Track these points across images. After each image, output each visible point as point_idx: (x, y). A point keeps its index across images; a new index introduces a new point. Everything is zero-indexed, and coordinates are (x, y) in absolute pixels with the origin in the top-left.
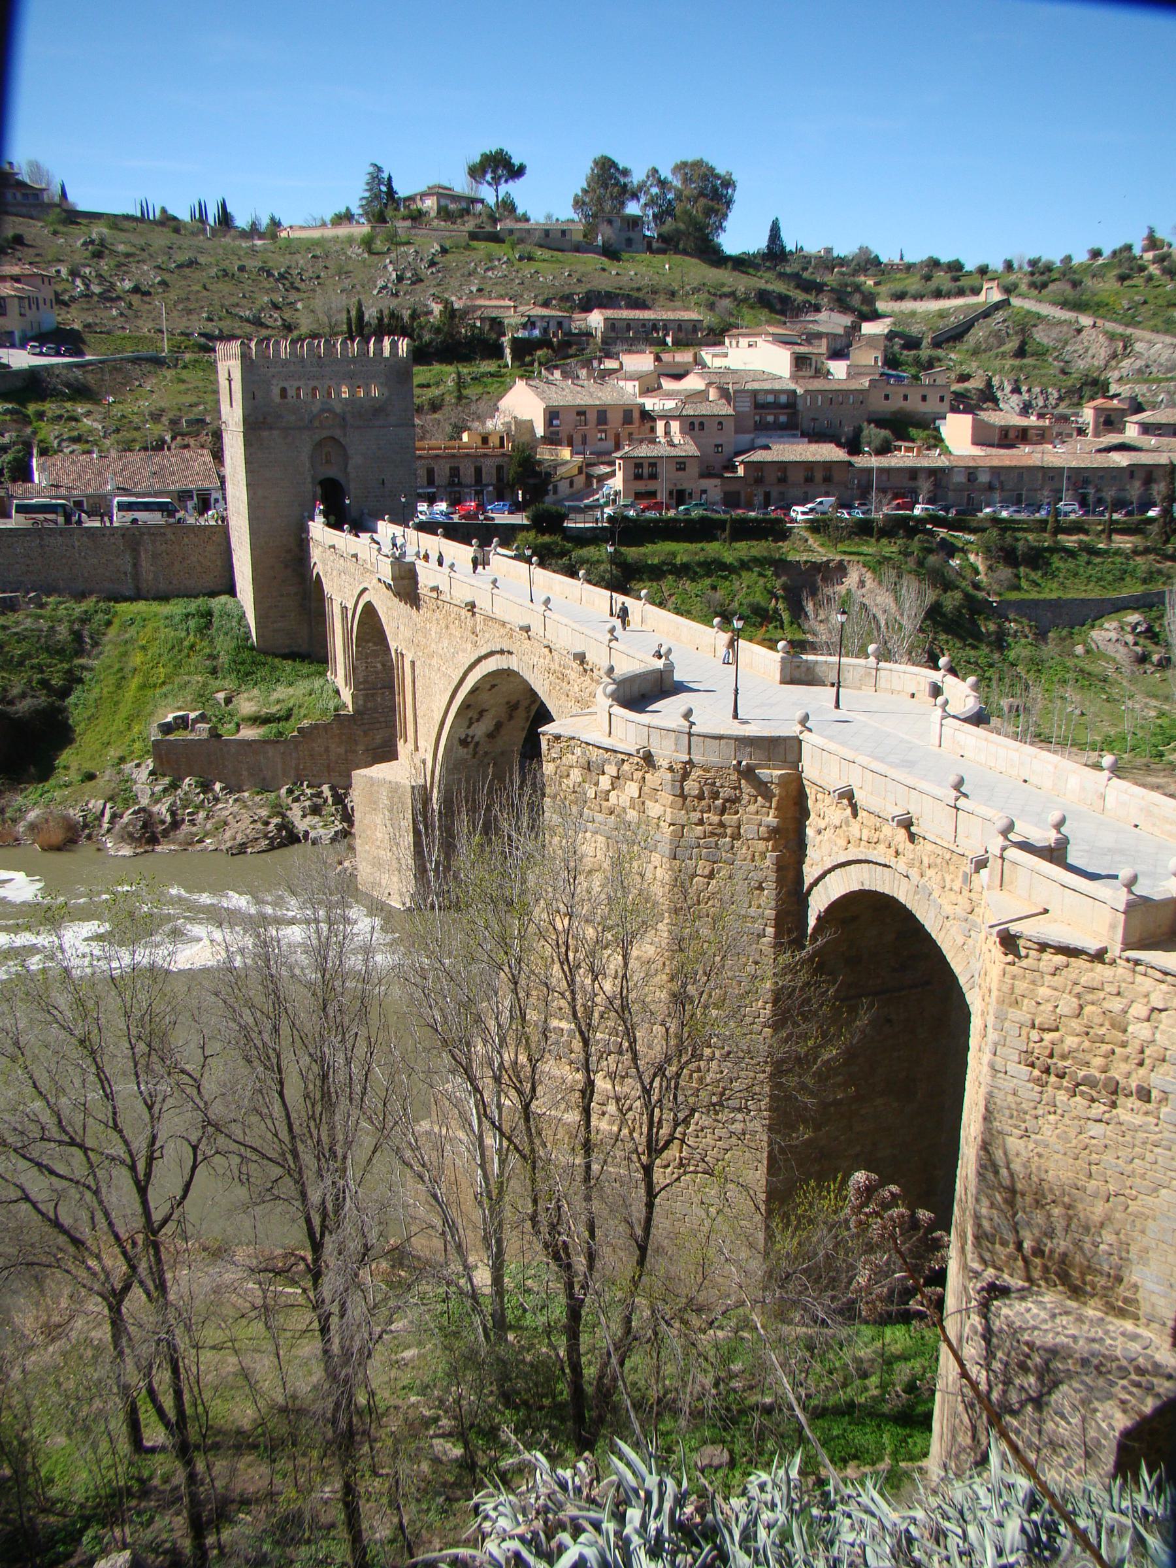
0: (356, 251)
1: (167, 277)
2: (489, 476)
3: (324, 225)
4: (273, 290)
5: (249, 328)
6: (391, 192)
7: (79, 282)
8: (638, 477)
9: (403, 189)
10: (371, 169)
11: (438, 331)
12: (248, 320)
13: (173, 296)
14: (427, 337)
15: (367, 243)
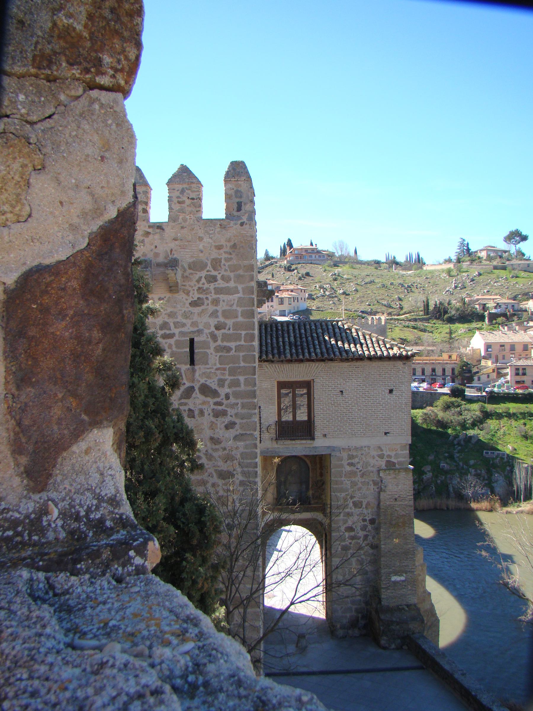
0: (444, 275)
1: (359, 288)
2: (448, 372)
3: (440, 264)
4: (402, 293)
5: (384, 309)
6: (468, 250)
7: (322, 291)
8: (517, 374)
9: (473, 249)
10: (460, 240)
11: (458, 310)
12: (385, 306)
13: (358, 296)
14: (453, 312)
15: (449, 272)
